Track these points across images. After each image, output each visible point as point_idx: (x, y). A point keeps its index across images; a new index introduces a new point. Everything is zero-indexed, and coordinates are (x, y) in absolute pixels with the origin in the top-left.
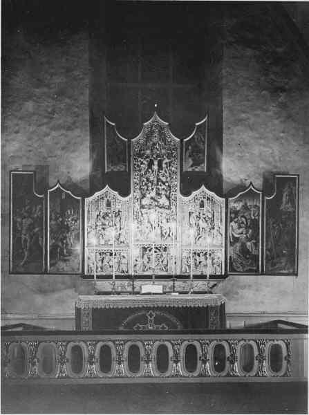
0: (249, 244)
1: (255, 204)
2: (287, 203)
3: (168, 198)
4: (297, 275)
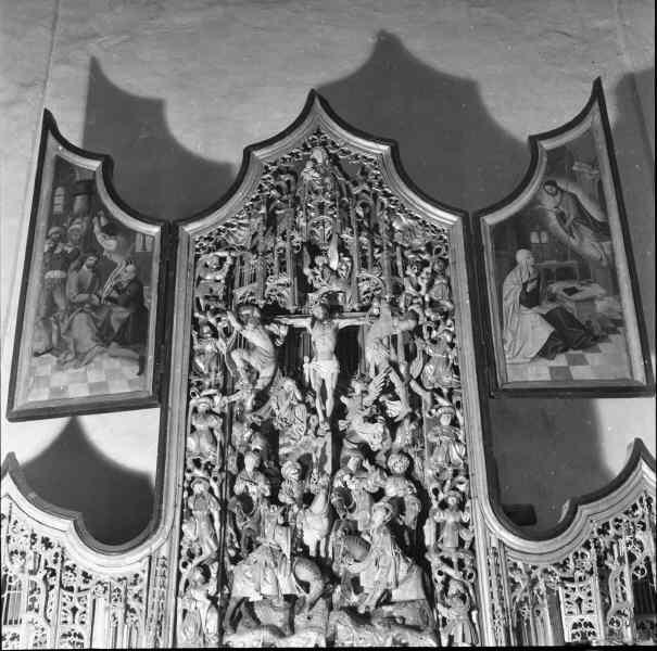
3: (411, 547)
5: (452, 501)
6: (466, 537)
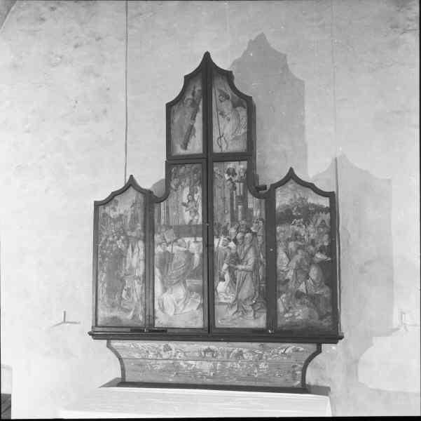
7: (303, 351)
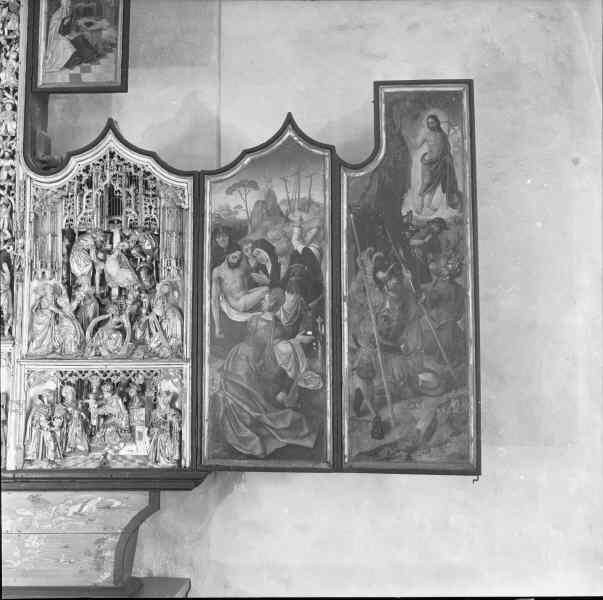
0: (284, 347)
1: (304, 195)
2: (429, 188)
4: (476, 471)
5: (7, 154)
6: (11, 173)
7: (119, 508)
